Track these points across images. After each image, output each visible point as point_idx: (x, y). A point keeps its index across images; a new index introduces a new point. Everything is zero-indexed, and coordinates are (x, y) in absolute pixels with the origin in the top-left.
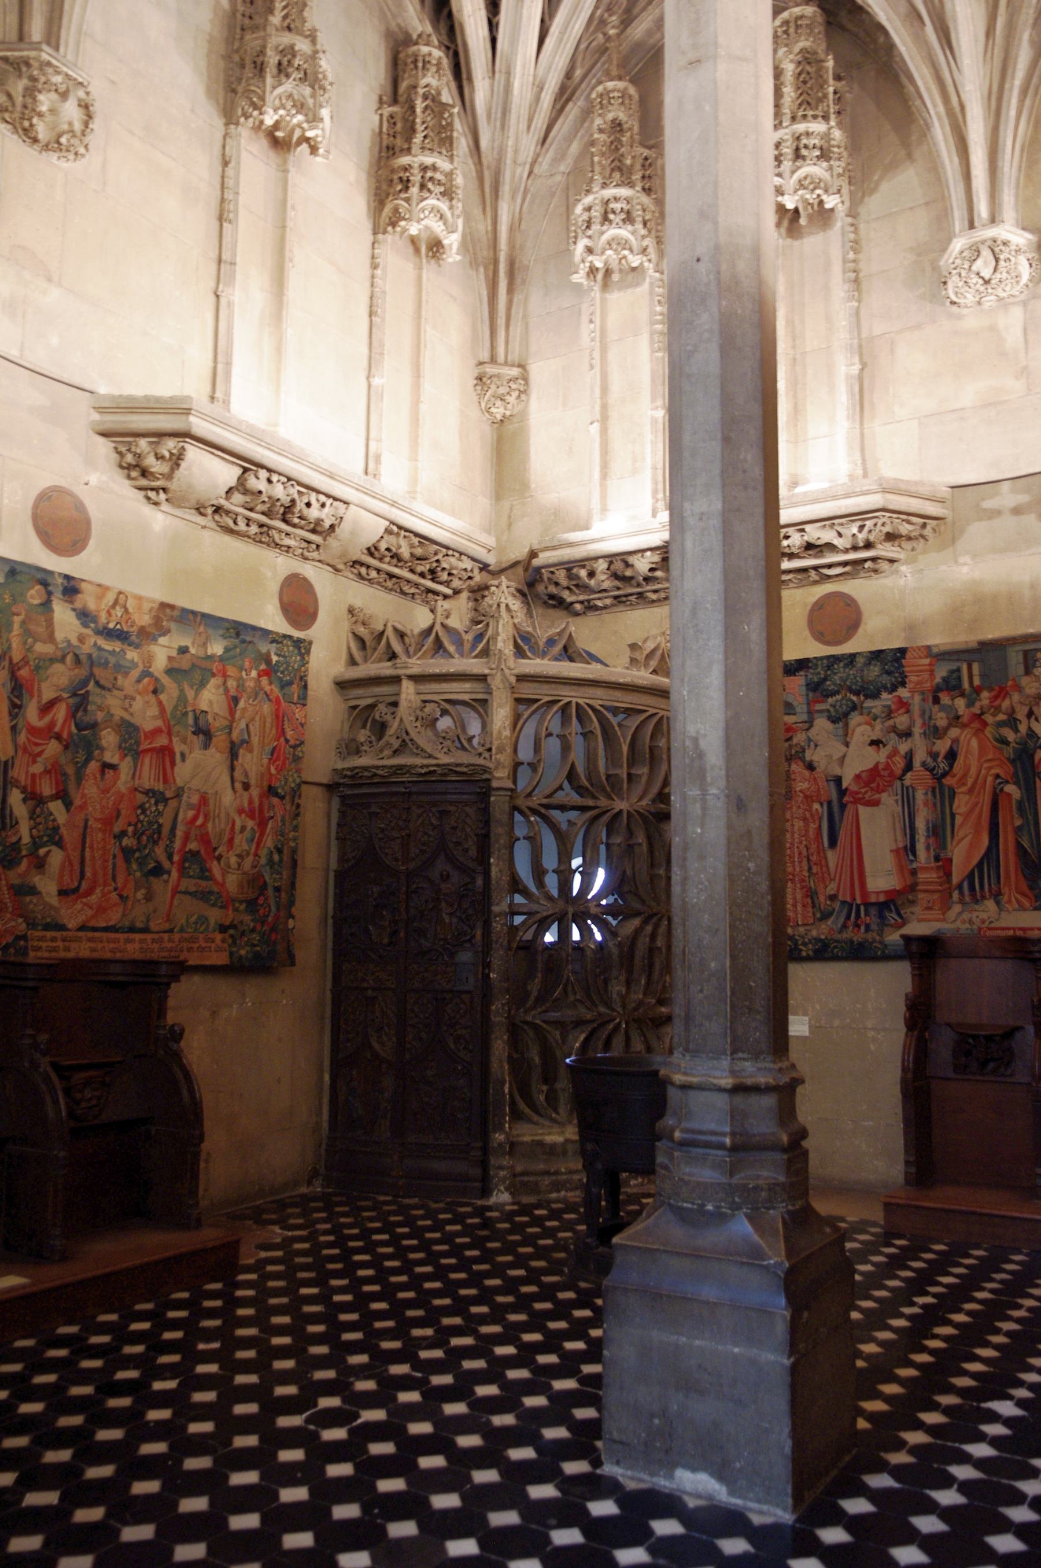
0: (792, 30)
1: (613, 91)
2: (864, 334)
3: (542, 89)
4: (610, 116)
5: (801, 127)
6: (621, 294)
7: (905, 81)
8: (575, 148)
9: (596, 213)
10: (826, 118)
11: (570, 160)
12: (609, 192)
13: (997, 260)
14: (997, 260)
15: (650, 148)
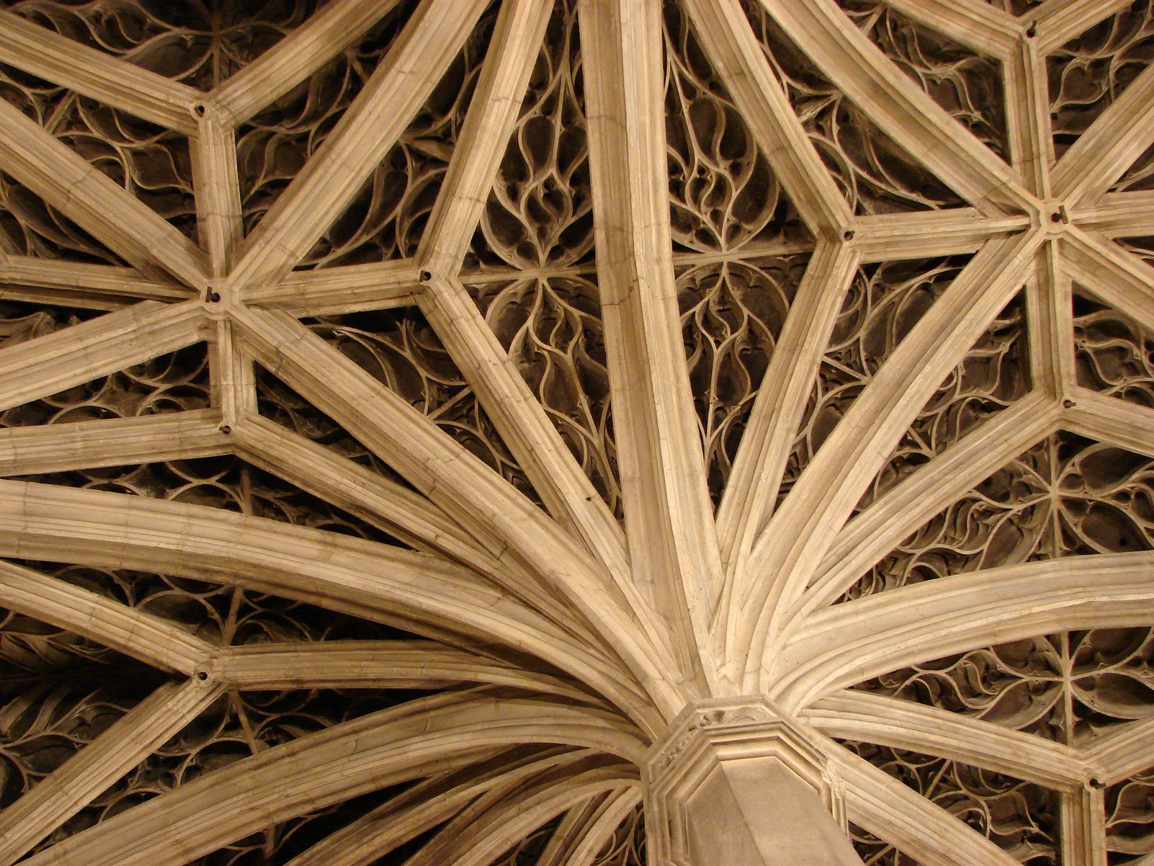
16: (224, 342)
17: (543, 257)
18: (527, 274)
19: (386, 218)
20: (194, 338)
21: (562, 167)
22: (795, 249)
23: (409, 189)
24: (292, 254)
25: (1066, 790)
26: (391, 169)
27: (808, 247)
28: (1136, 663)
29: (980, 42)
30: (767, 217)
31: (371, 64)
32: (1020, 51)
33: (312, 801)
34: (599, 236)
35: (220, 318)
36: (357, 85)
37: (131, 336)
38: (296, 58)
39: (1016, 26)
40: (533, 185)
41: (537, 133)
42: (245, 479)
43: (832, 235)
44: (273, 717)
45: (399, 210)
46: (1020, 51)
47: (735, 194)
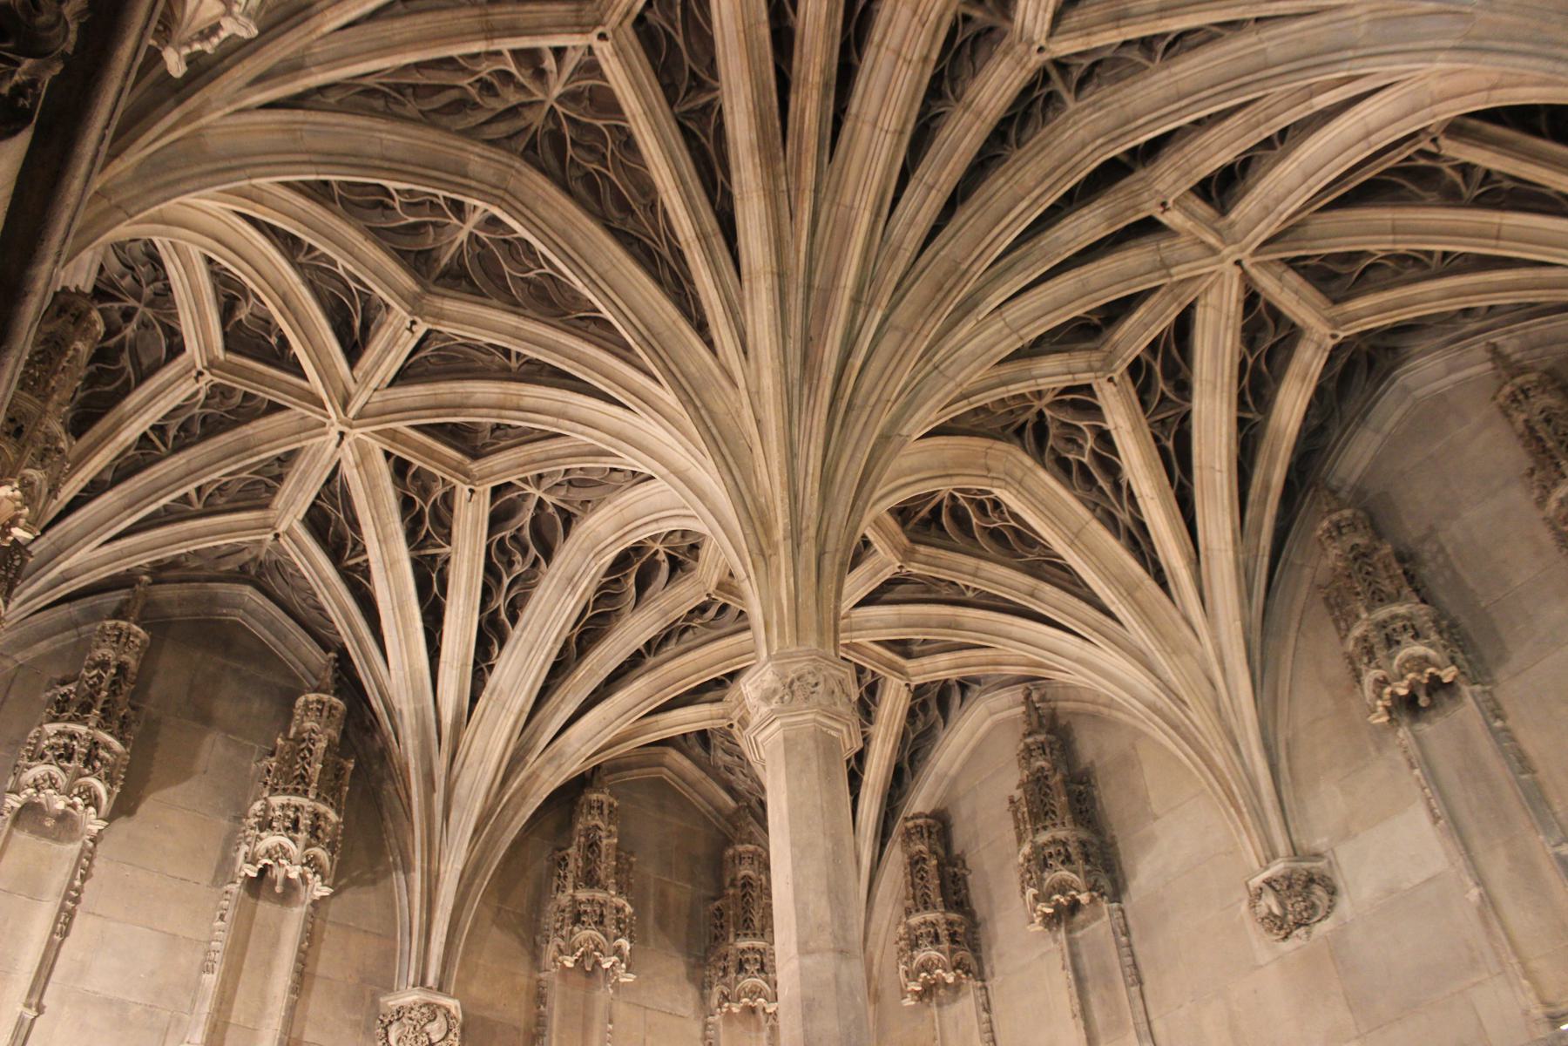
0: (325, 714)
1: (136, 636)
2: (294, 1035)
3: (67, 580)
4: (124, 657)
5: (322, 808)
6: (32, 838)
7: (387, 815)
8: (42, 647)
9: (80, 748)
10: (338, 813)
11: (30, 654)
12: (104, 736)
13: (449, 1031)
14: (449, 1031)
15: (133, 708)
16: (1211, 239)
17: (1048, 413)
18: (1048, 398)
19: (1163, 375)
20: (1233, 216)
21: (1081, 465)
22: (916, 520)
23: (1161, 385)
24: (1205, 306)
25: (474, 467)
26: (1181, 376)
27: (910, 526)
28: (520, 529)
29: (925, 661)
30: (945, 519)
31: (1241, 422)
32: (902, 672)
33: (879, 46)
34: (1028, 461)
35: (1226, 251)
36: (1242, 404)
37: (1281, 208)
38: (1291, 405)
39: (917, 680)
40: (1090, 443)
41: (1112, 468)
42: (1125, 159)
43: (908, 555)
44: (958, 41)
45: (1157, 368)
46: (902, 672)
47: (974, 520)
